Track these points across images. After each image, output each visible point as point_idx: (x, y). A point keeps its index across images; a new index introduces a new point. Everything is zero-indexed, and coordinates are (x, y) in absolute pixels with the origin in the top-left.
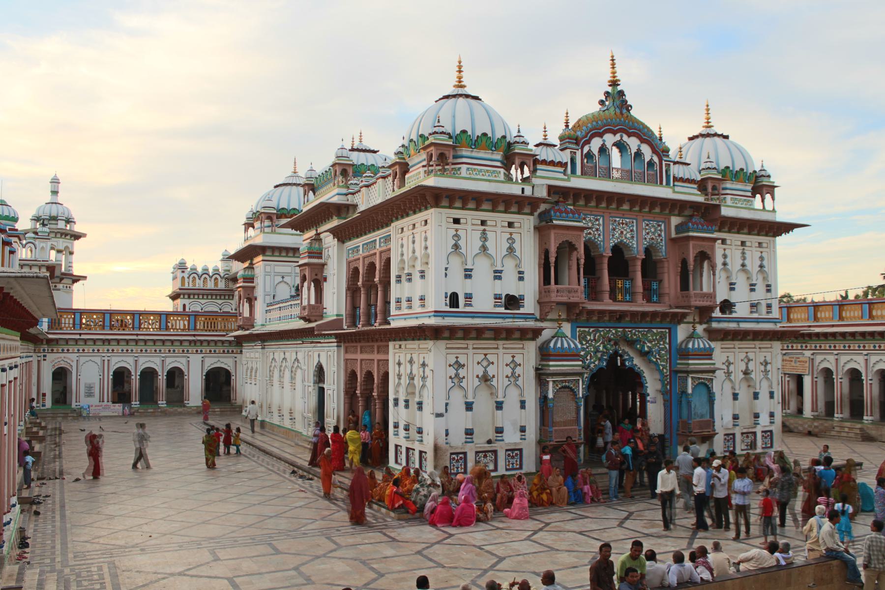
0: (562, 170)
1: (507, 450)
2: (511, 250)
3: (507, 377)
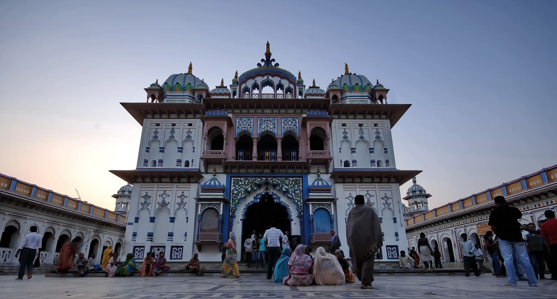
1: (172, 247)
3: (178, 203)
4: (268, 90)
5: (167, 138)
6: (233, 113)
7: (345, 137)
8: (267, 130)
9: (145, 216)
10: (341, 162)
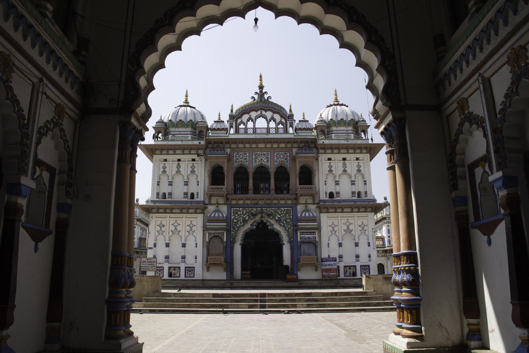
0: (225, 132)
1: (186, 268)
2: (193, 172)
3: (187, 231)
4: (261, 123)
5: (174, 172)
6: (230, 148)
7: (330, 171)
8: (262, 164)
9: (161, 244)
10: (326, 193)
